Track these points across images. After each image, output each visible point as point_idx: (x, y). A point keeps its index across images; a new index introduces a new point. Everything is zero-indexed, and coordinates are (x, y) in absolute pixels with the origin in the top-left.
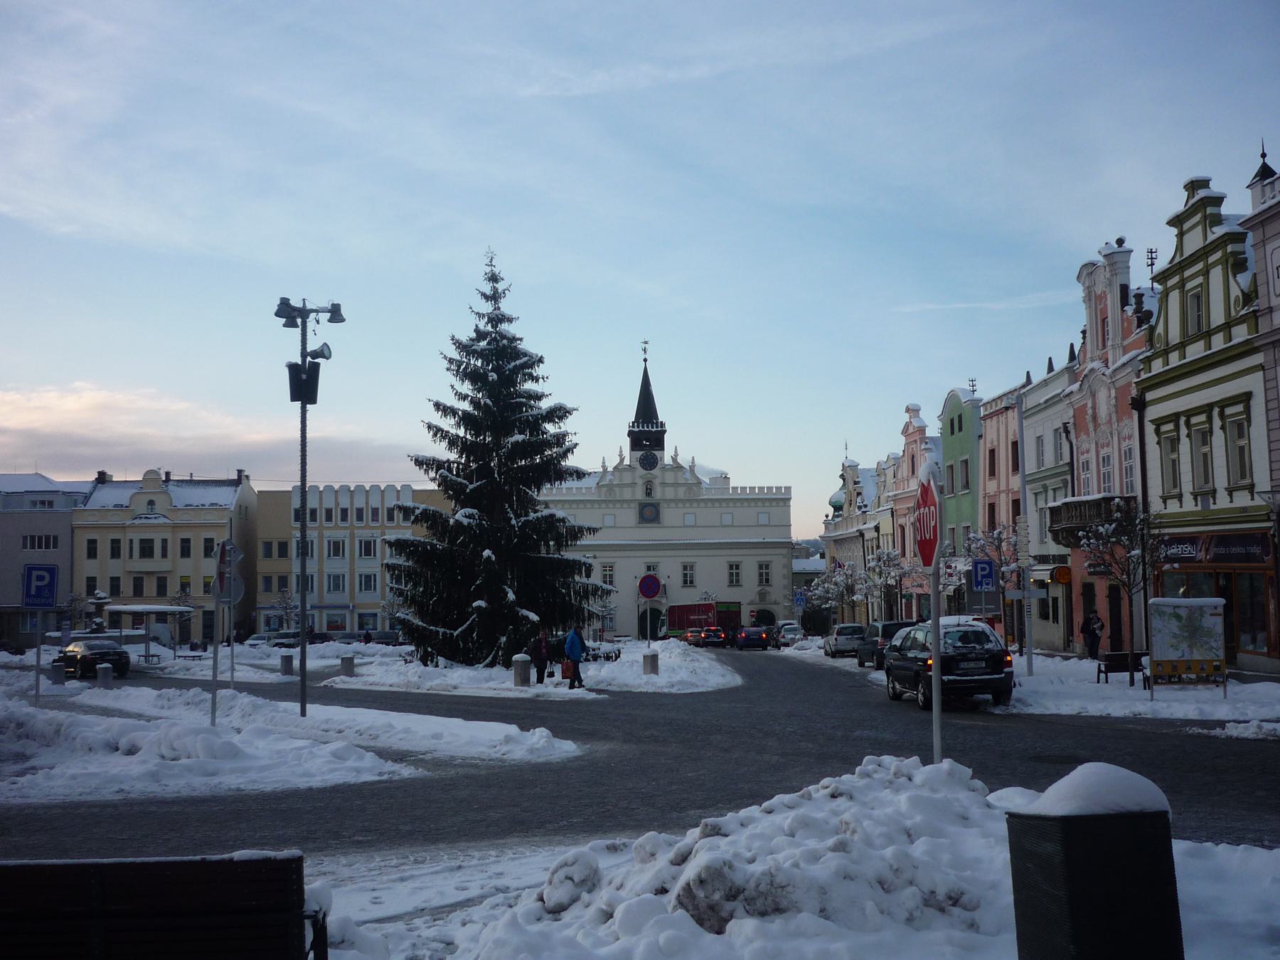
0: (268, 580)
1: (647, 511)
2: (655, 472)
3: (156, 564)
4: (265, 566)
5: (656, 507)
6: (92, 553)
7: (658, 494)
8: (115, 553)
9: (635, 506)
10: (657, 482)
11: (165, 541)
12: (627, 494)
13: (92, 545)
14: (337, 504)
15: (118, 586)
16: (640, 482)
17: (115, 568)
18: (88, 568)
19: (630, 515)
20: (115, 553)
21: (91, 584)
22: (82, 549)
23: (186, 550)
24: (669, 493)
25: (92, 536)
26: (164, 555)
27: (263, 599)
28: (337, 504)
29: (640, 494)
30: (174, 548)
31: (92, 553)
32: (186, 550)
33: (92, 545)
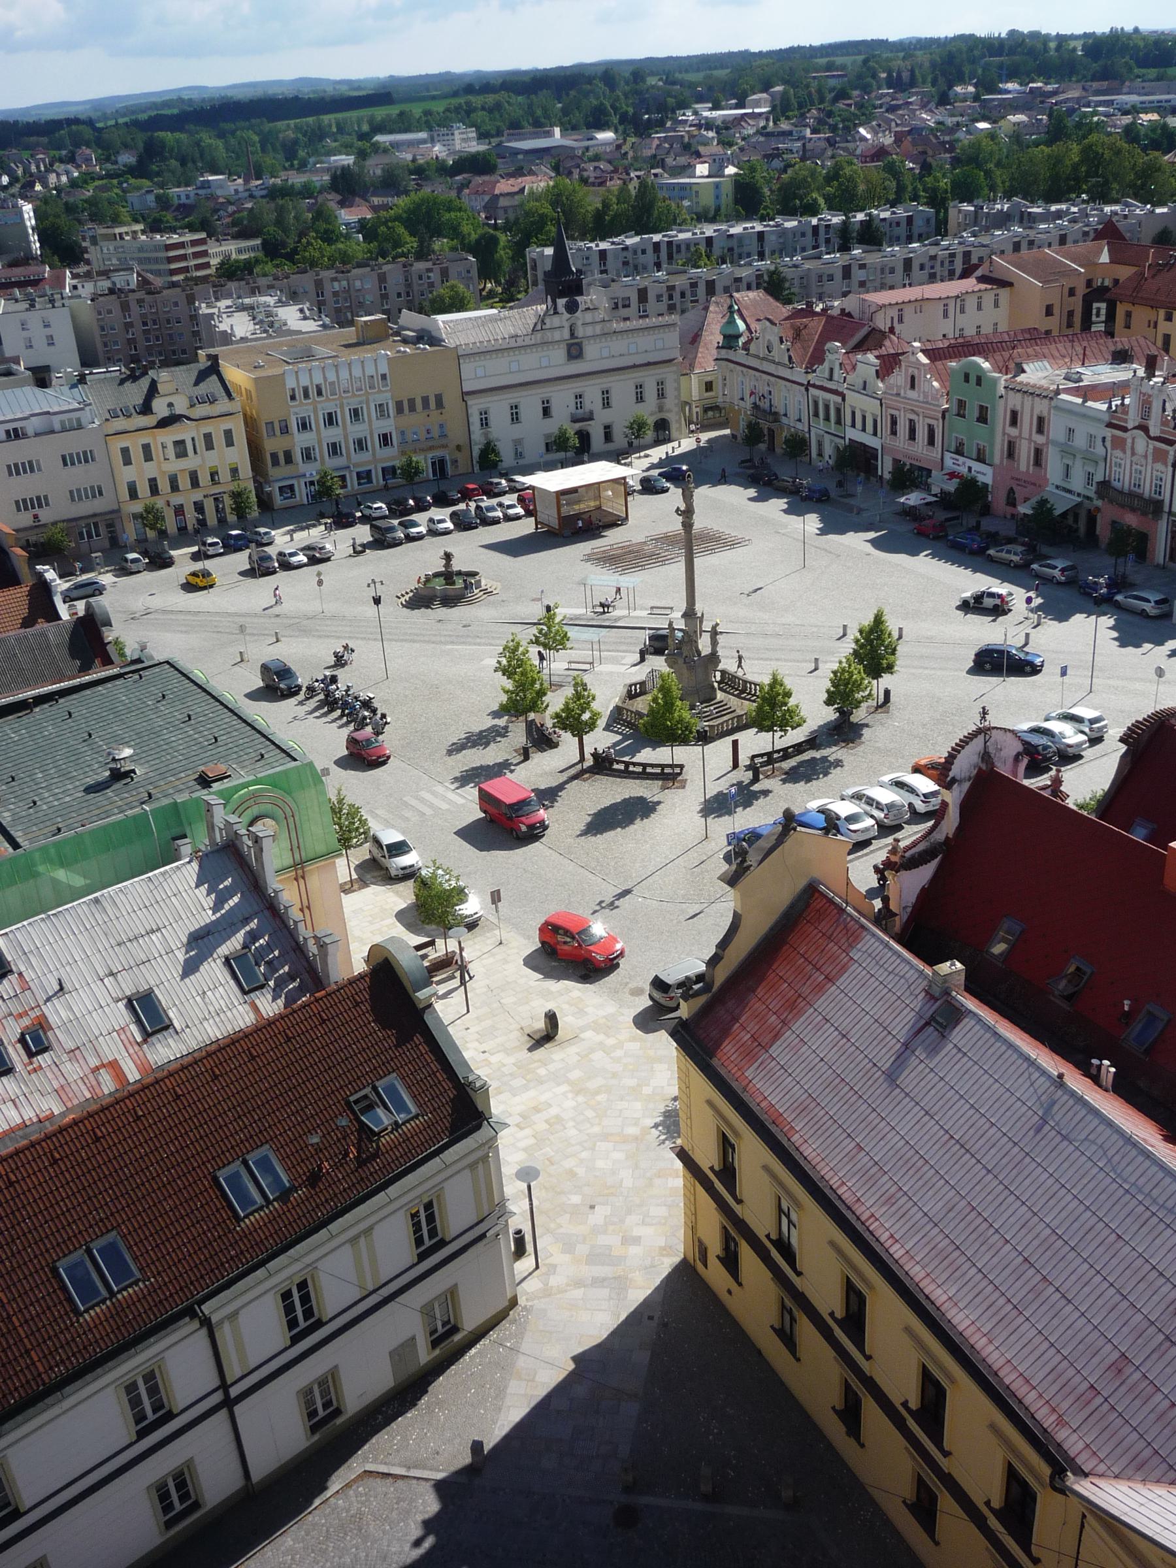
0: (274, 456)
1: (574, 352)
2: (578, 314)
3: (190, 463)
4: (271, 445)
5: (579, 346)
6: (127, 461)
7: (580, 332)
8: (148, 455)
9: (563, 346)
10: (579, 323)
11: (193, 439)
12: (557, 335)
13: (125, 452)
14: (325, 379)
15: (156, 485)
16: (567, 325)
17: (151, 470)
18: (127, 474)
19: (559, 354)
20: (148, 457)
21: (133, 494)
22: (118, 458)
23: (209, 446)
24: (589, 331)
25: (124, 445)
26: (195, 452)
27: (273, 472)
28: (325, 379)
29: (566, 334)
30: (201, 444)
31: (127, 461)
32: (209, 446)
33: (125, 452)
